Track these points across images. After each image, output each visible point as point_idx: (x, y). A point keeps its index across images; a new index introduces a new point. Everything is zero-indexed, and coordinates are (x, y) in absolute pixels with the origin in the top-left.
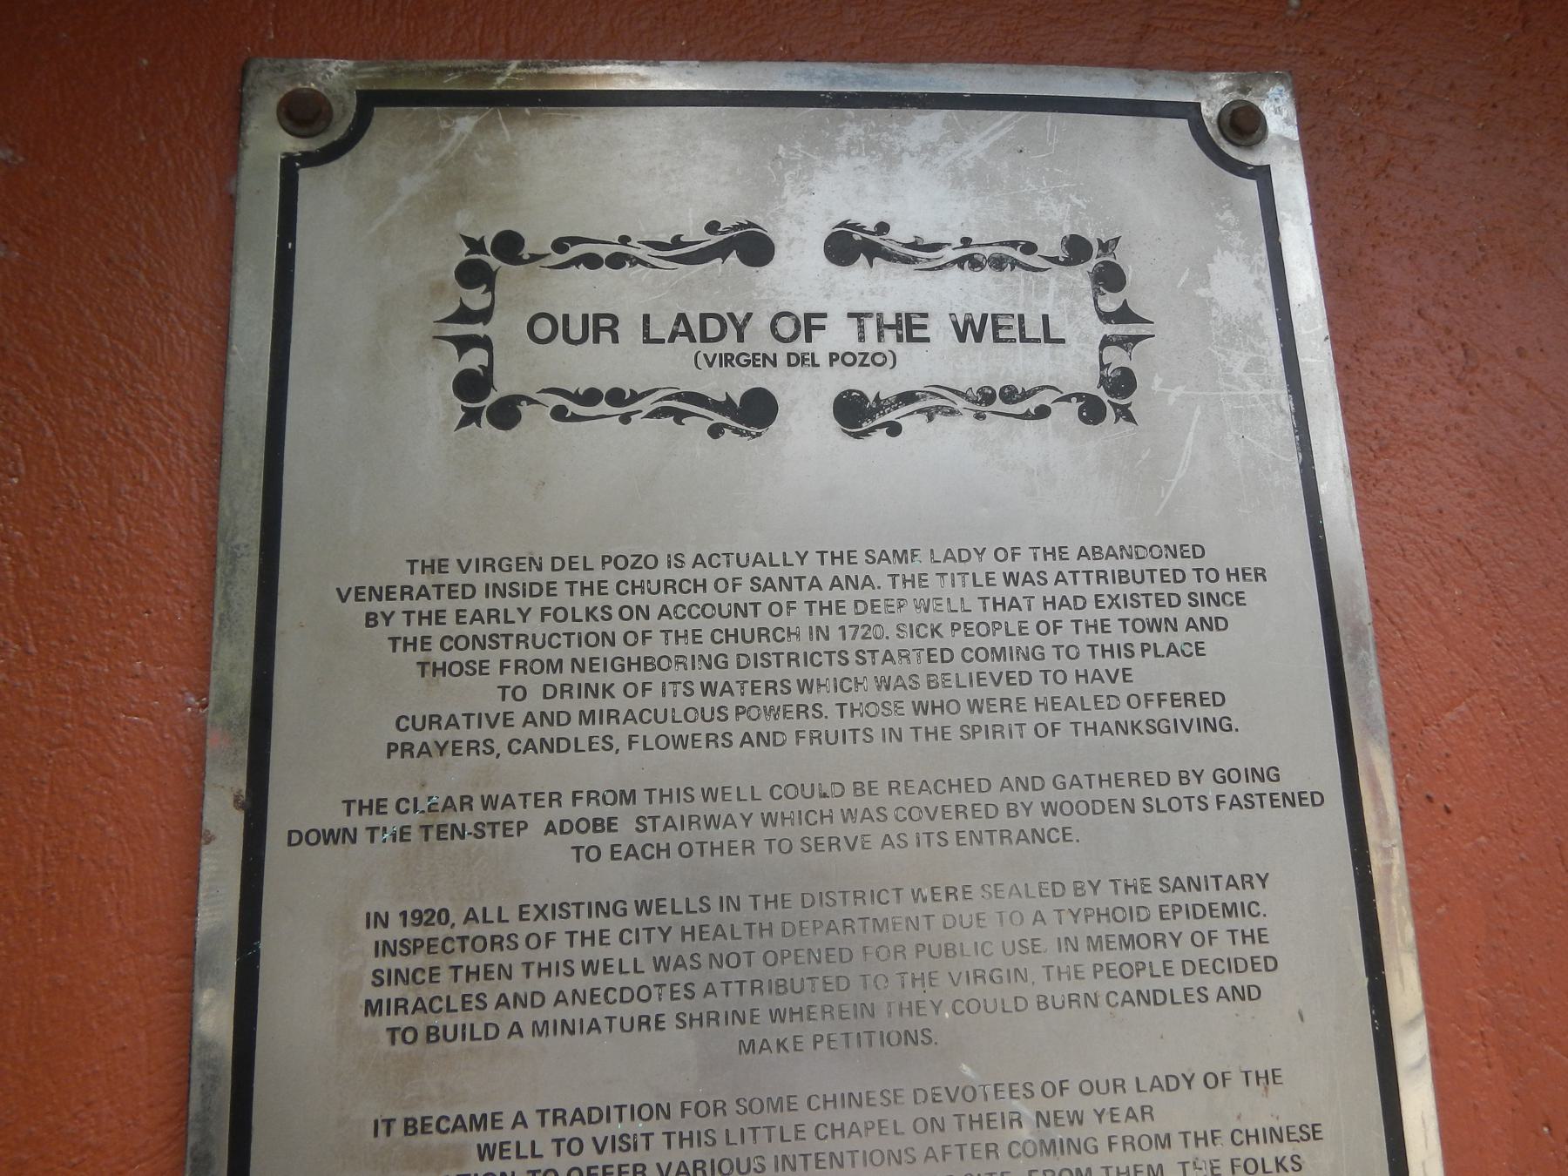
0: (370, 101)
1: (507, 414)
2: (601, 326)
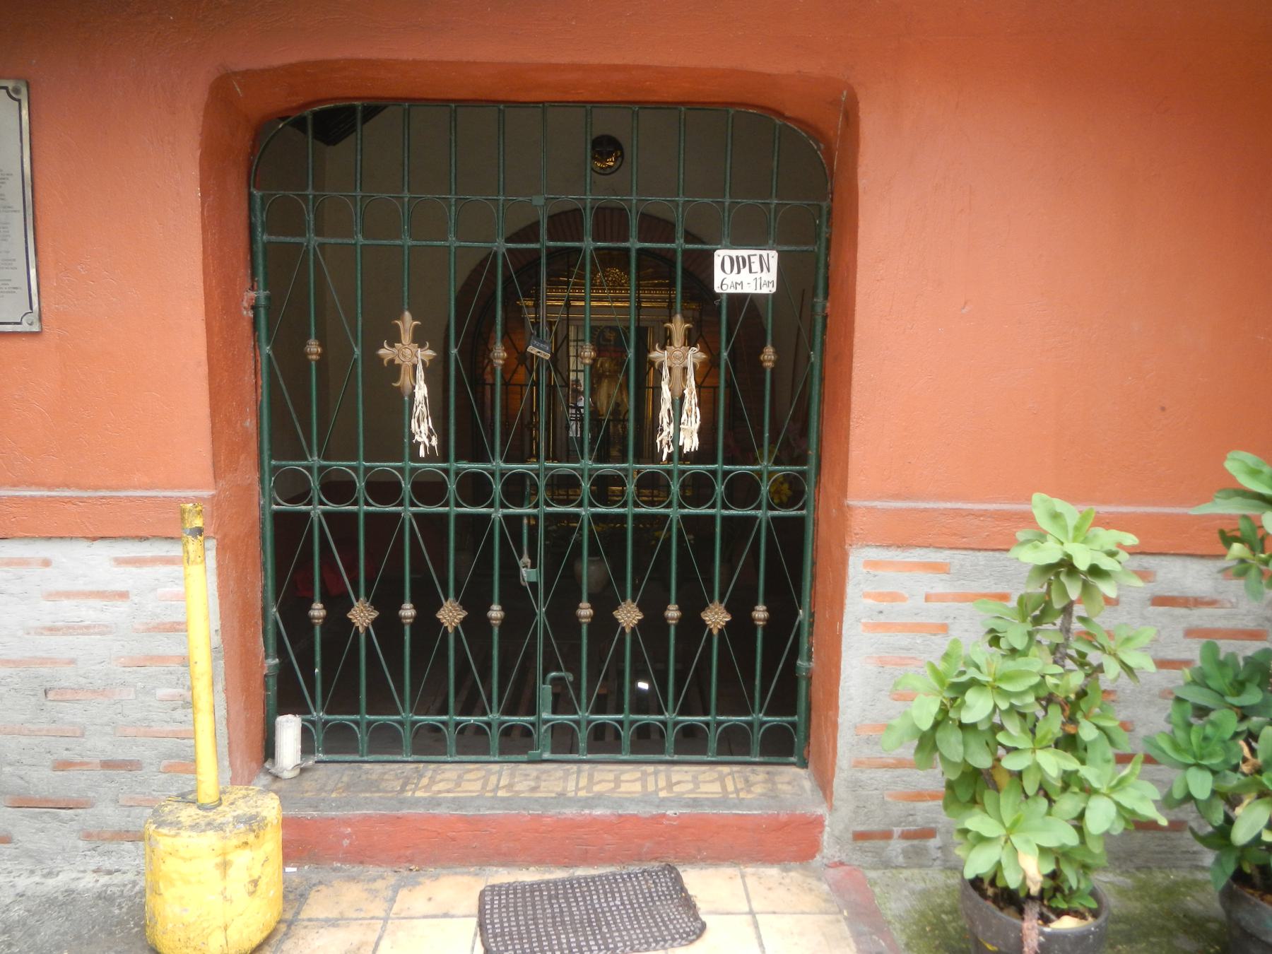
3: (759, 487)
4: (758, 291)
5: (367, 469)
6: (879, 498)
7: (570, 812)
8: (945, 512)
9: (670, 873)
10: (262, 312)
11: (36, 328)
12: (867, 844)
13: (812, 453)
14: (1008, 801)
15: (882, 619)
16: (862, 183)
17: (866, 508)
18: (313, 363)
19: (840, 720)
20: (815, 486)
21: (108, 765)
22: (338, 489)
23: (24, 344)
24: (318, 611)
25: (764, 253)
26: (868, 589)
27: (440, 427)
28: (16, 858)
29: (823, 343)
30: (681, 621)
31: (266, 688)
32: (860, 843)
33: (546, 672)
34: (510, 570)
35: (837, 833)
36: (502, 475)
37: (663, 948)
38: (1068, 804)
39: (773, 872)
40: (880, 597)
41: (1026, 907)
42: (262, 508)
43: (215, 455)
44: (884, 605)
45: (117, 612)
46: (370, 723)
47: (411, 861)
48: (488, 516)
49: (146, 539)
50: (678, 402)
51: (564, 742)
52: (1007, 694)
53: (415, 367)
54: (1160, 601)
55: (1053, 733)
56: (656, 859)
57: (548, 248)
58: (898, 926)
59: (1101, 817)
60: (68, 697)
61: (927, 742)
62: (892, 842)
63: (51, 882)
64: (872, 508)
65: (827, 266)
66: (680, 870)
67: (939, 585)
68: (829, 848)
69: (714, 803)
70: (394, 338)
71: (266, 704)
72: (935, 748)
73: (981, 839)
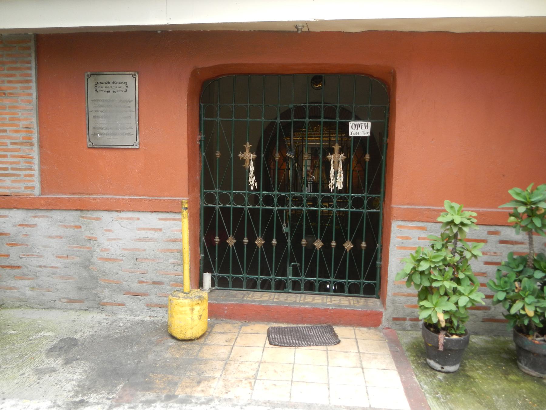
0: (91, 75)
1: (98, 92)
2: (102, 87)
3: (364, 202)
4: (364, 135)
5: (234, 193)
6: (402, 205)
7: (297, 306)
8: (425, 210)
9: (330, 327)
10: (203, 142)
11: (138, 147)
12: (397, 322)
13: (382, 190)
14: (435, 298)
15: (403, 245)
16: (397, 100)
17: (398, 208)
18: (218, 159)
19: (388, 279)
20: (383, 202)
21: (154, 283)
22: (224, 199)
23: (134, 152)
24: (217, 239)
25: (366, 123)
26: (398, 235)
27: (257, 180)
28: (126, 311)
29: (386, 153)
30: (336, 246)
31: (200, 264)
32: (395, 322)
33: (290, 263)
34: (279, 228)
35: (387, 318)
36: (277, 196)
37: (326, 345)
38: (454, 298)
39: (365, 329)
40: (403, 238)
41: (441, 332)
42: (201, 205)
43: (189, 187)
44: (404, 241)
45: (158, 235)
46: (233, 277)
47: (246, 319)
48: (272, 209)
49: (168, 212)
50: (336, 173)
51: (296, 286)
52: (434, 263)
53: (250, 160)
54: (502, 242)
55: (449, 276)
56: (326, 323)
57: (294, 122)
58: (405, 345)
59: (463, 301)
60: (143, 261)
61: (410, 278)
62: (406, 322)
63: (137, 318)
64: (400, 208)
65: (388, 127)
66: (333, 327)
67: (423, 234)
68: (384, 322)
69: (345, 306)
70: (244, 151)
71: (200, 269)
72: (412, 281)
73: (426, 308)
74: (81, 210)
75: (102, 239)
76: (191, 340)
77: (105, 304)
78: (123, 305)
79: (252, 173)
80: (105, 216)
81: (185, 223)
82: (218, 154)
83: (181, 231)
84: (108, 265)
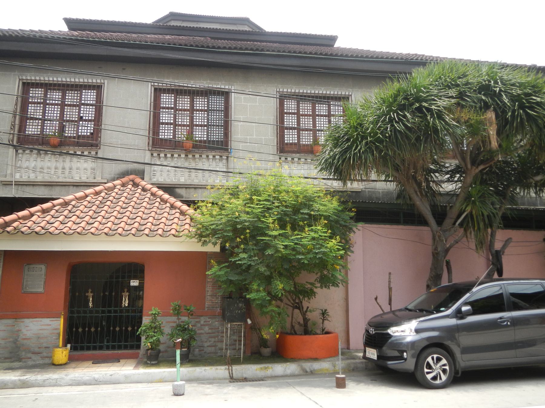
21: (46, 347)
22: (79, 312)
27: (93, 304)
34: (102, 323)
51: (108, 348)
59: (155, 338)
68: (140, 356)
70: (88, 292)
74: (16, 319)
75: (24, 331)
76: (61, 365)
77: (22, 359)
78: (30, 358)
79: (91, 301)
80: (27, 321)
81: (62, 320)
82: (77, 294)
83: (60, 325)
84: (25, 341)
